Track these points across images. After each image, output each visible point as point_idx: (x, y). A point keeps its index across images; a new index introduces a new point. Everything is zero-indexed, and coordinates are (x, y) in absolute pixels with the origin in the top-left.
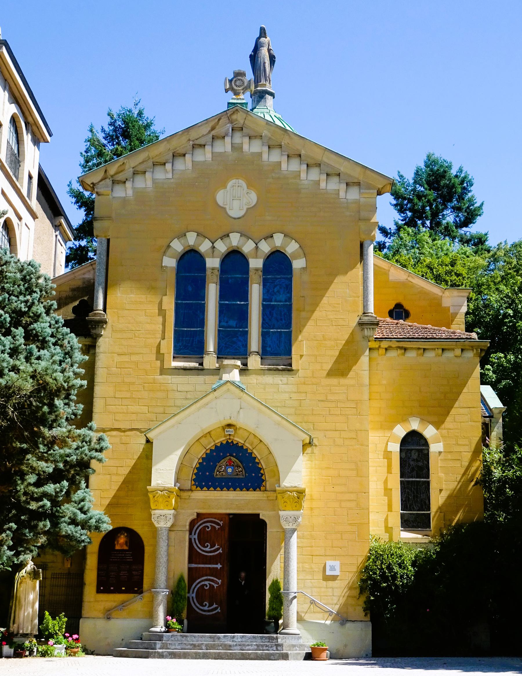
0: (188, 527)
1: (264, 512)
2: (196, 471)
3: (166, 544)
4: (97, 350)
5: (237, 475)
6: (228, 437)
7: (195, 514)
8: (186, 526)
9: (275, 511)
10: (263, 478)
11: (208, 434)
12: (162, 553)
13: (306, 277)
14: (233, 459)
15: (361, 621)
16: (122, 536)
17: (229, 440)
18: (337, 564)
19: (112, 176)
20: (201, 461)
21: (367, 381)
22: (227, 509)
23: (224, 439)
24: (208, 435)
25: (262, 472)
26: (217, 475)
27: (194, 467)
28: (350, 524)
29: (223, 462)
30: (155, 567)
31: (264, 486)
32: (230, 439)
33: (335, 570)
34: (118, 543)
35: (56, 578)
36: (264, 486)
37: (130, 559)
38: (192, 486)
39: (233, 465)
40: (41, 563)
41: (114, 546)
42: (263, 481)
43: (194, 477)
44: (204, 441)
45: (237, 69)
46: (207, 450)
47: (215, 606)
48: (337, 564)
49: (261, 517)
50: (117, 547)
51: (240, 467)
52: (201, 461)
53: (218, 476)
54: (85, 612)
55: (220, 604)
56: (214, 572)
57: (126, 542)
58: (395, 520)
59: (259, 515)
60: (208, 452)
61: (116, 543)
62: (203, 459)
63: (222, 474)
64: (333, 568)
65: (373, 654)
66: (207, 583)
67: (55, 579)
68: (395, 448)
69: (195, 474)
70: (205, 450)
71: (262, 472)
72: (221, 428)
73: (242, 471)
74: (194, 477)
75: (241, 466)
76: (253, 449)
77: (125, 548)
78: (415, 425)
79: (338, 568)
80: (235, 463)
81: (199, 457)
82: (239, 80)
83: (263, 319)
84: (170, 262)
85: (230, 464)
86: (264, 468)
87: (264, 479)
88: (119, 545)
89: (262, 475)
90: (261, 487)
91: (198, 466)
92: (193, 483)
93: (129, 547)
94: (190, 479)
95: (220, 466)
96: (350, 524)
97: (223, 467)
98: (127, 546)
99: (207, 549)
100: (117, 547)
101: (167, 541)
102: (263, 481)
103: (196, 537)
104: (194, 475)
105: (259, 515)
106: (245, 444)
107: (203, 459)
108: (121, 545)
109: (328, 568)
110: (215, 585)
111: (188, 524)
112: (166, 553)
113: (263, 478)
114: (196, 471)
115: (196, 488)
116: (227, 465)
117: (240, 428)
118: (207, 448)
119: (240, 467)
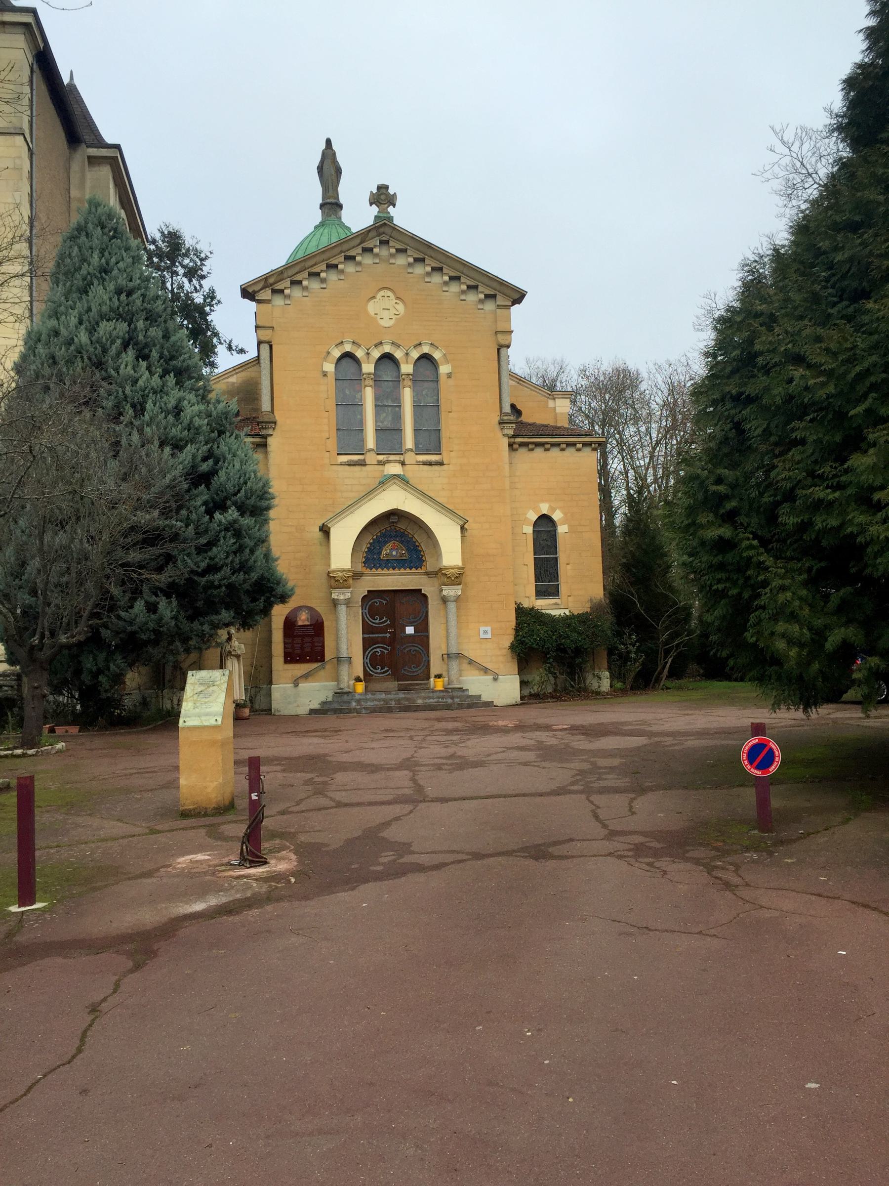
1: (426, 588)
4: (269, 449)
13: (451, 382)
18: (489, 629)
19: (271, 285)
20: (369, 546)
21: (507, 473)
25: (422, 553)
29: (390, 545)
30: (337, 638)
45: (381, 182)
47: (386, 669)
48: (489, 629)
49: (423, 592)
52: (369, 546)
55: (390, 667)
56: (383, 641)
57: (308, 618)
58: (531, 590)
59: (420, 590)
60: (375, 537)
62: (371, 544)
64: (485, 632)
66: (378, 650)
68: (529, 530)
71: (422, 553)
74: (364, 560)
77: (307, 623)
78: (544, 509)
79: (489, 632)
82: (382, 194)
83: (415, 420)
84: (330, 367)
91: (366, 550)
99: (377, 621)
100: (300, 623)
103: (367, 611)
105: (420, 590)
107: (371, 544)
108: (304, 621)
109: (482, 632)
110: (386, 652)
113: (423, 558)
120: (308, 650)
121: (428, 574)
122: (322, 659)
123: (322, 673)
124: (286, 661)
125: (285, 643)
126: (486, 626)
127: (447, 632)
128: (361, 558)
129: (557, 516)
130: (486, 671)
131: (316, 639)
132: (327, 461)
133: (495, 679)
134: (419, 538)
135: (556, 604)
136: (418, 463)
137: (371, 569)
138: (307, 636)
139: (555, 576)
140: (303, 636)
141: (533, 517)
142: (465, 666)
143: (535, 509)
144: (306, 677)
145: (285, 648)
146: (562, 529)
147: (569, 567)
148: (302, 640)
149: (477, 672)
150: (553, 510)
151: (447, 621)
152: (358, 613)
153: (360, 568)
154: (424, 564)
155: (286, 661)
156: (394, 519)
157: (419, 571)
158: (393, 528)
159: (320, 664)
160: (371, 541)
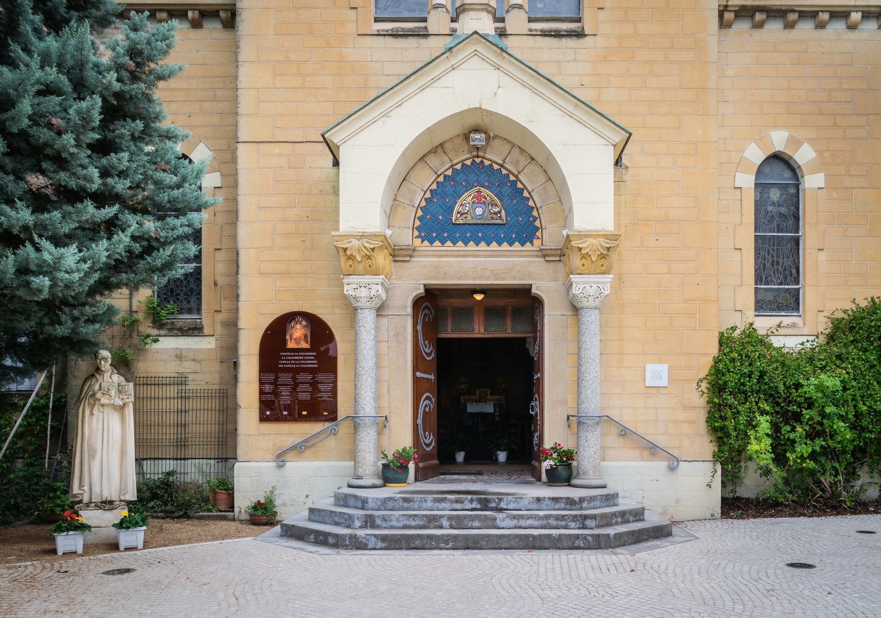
0: (409, 310)
2: (420, 213)
3: (372, 336)
5: (493, 218)
6: (474, 153)
7: (422, 287)
8: (406, 307)
9: (558, 280)
10: (537, 223)
11: (440, 148)
12: (365, 352)
14: (485, 192)
15: (703, 461)
16: (298, 326)
17: (476, 159)
20: (428, 195)
22: (475, 279)
23: (468, 156)
24: (440, 150)
25: (535, 213)
26: (457, 219)
27: (416, 205)
28: (686, 301)
29: (467, 198)
31: (538, 238)
32: (478, 157)
33: (661, 378)
34: (291, 338)
35: (182, 397)
36: (538, 238)
37: (313, 364)
38: (414, 239)
39: (484, 203)
40: (176, 375)
41: (284, 342)
42: (537, 229)
43: (418, 223)
44: (433, 160)
46: (439, 176)
49: (534, 291)
50: (291, 345)
51: (496, 205)
52: (428, 195)
53: (461, 222)
54: (241, 452)
57: (306, 336)
58: (747, 296)
61: (288, 337)
63: (466, 217)
65: (722, 514)
67: (183, 400)
69: (419, 218)
70: (436, 176)
71: (535, 213)
72: (461, 138)
73: (500, 212)
74: (418, 223)
75: (499, 203)
76: (519, 173)
77: (304, 345)
78: (779, 141)
80: (488, 198)
81: (425, 189)
85: (479, 199)
86: (539, 206)
87: (539, 226)
88: (293, 341)
89: (535, 219)
90: (534, 240)
91: (423, 204)
92: (416, 233)
93: (311, 345)
94: (411, 226)
95: (462, 205)
96: (686, 301)
97: (468, 205)
98: (307, 342)
100: (291, 345)
101: (373, 332)
102: (537, 229)
104: (417, 220)
106: (505, 165)
108: (297, 340)
111: (409, 304)
112: (372, 353)
113: (537, 223)
114: (420, 213)
115: (422, 243)
116: (473, 202)
117: (496, 137)
118: (439, 173)
119: (496, 205)
120: (304, 396)
121: (544, 254)
122: (333, 417)
123: (331, 443)
124: (263, 419)
125: (261, 383)
126: (660, 362)
127: (579, 371)
128: (408, 217)
129: (804, 156)
130: (653, 450)
131: (320, 377)
132: (351, 28)
133: (672, 469)
134: (530, 180)
135: (794, 325)
136: (532, 34)
137: (431, 242)
138: (305, 370)
139: (793, 274)
140: (295, 371)
141: (756, 155)
142: (613, 439)
143: (761, 142)
144: (299, 449)
145: (262, 392)
146: (812, 182)
147: (822, 256)
148: (294, 379)
149: (636, 453)
150: (796, 143)
151: (579, 349)
152: (404, 328)
153: (406, 236)
154: (538, 234)
155: (263, 419)
156: (478, 139)
157: (528, 247)
158: (478, 160)
159: (327, 425)
160: (434, 187)
